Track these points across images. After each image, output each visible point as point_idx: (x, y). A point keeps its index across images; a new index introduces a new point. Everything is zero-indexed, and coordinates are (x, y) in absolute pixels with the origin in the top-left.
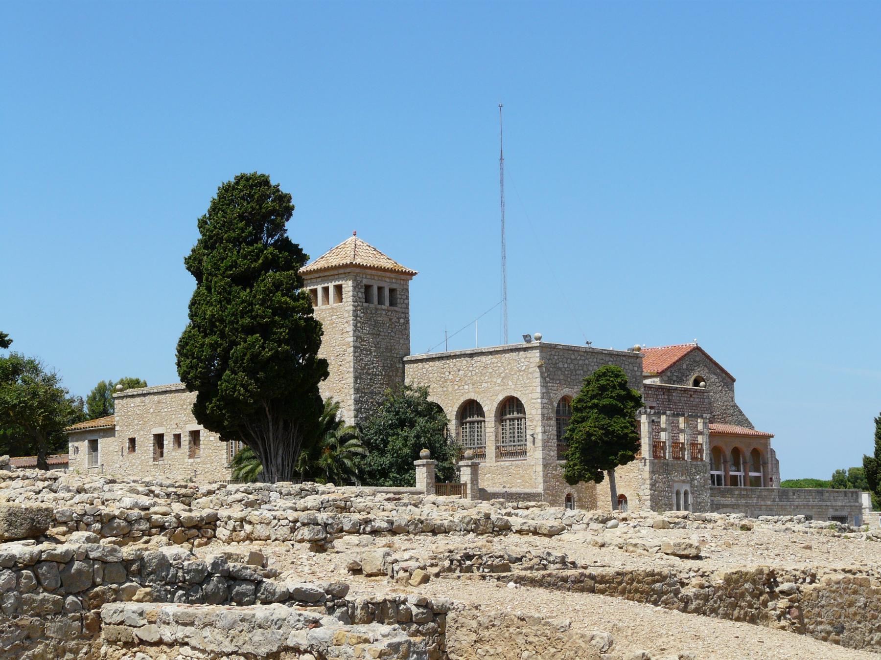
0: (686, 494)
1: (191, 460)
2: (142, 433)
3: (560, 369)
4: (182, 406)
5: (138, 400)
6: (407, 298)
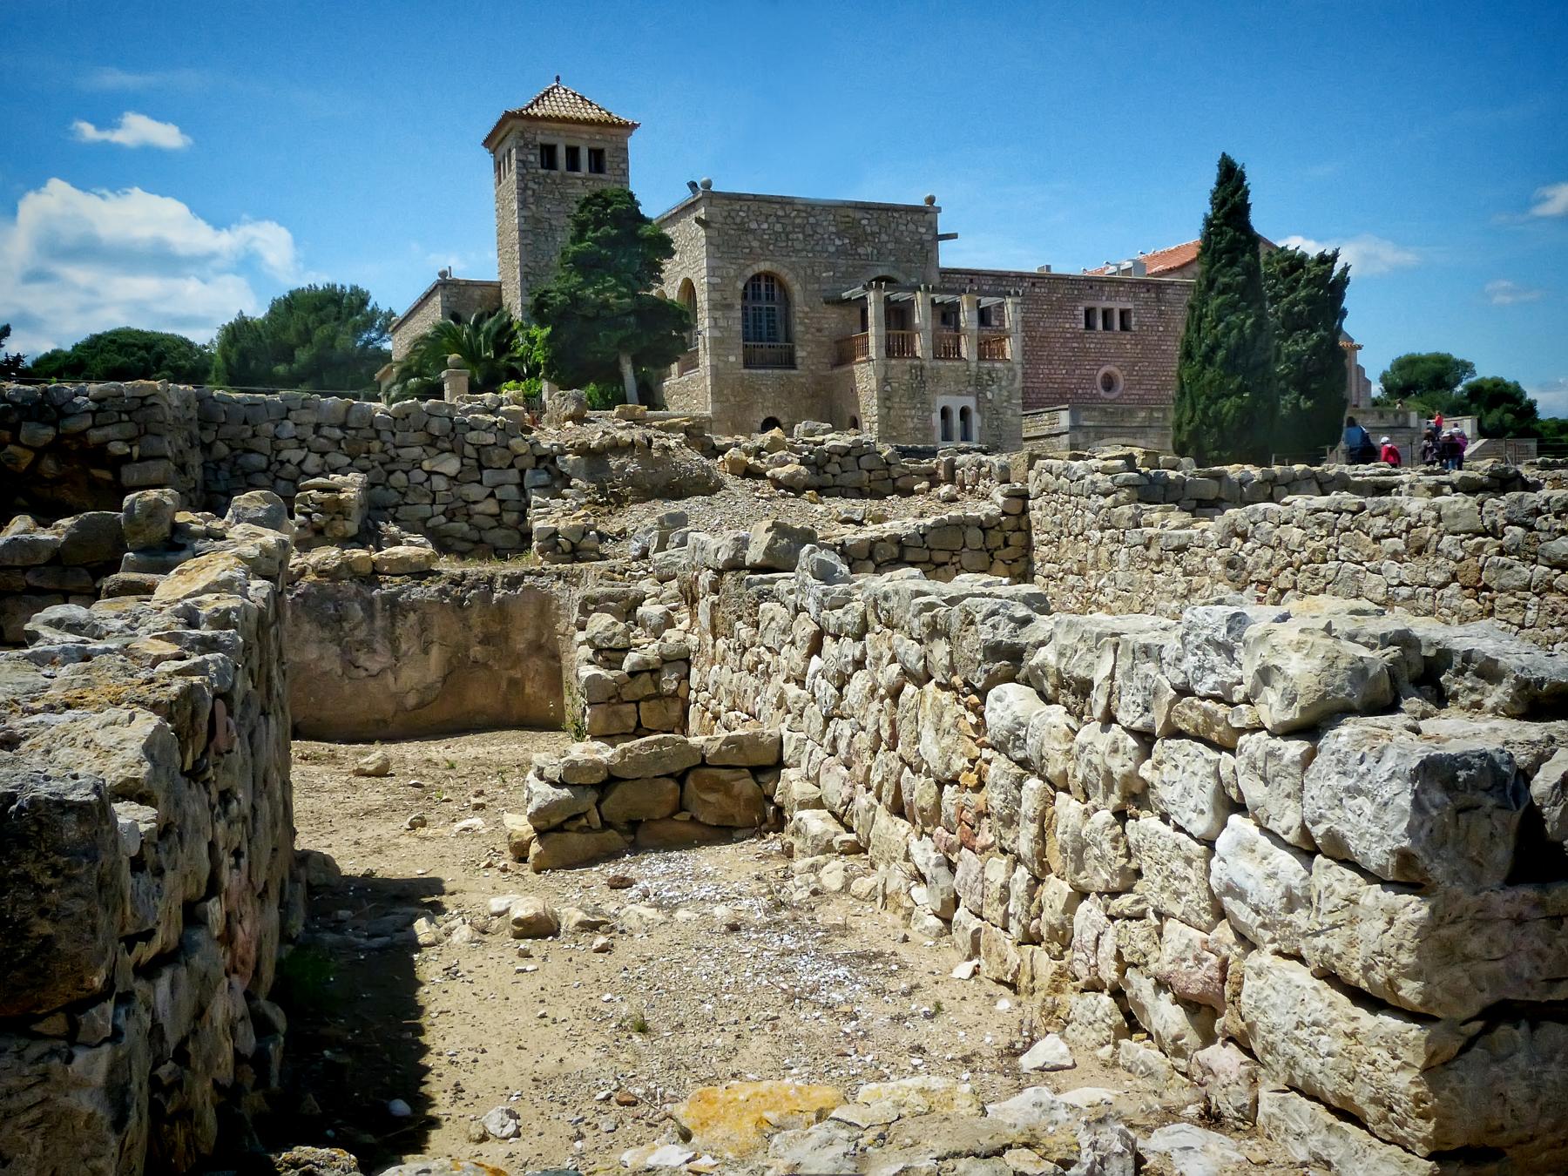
0: (964, 413)
3: (753, 231)
6: (626, 161)
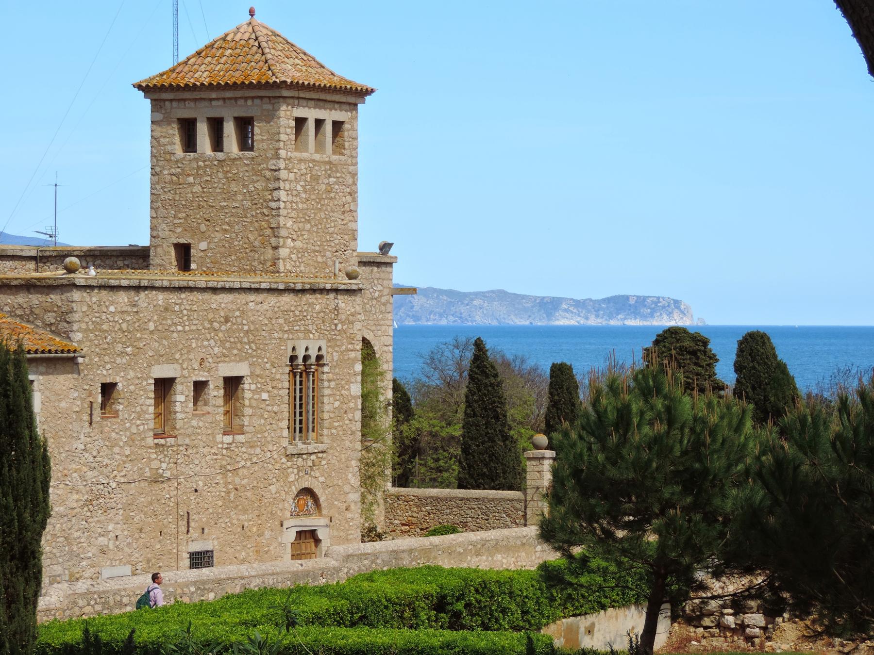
1: (228, 439)
2: (132, 374)
4: (211, 322)
5: (123, 297)
